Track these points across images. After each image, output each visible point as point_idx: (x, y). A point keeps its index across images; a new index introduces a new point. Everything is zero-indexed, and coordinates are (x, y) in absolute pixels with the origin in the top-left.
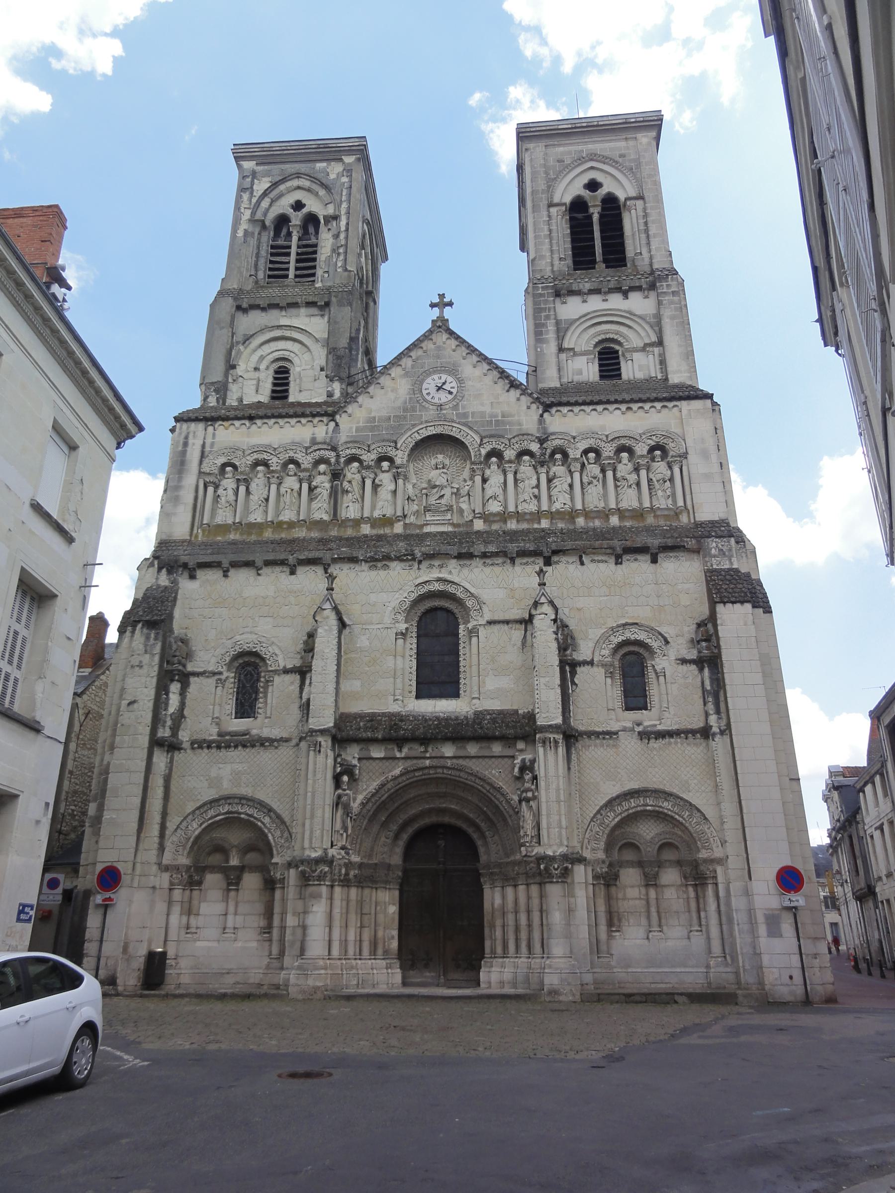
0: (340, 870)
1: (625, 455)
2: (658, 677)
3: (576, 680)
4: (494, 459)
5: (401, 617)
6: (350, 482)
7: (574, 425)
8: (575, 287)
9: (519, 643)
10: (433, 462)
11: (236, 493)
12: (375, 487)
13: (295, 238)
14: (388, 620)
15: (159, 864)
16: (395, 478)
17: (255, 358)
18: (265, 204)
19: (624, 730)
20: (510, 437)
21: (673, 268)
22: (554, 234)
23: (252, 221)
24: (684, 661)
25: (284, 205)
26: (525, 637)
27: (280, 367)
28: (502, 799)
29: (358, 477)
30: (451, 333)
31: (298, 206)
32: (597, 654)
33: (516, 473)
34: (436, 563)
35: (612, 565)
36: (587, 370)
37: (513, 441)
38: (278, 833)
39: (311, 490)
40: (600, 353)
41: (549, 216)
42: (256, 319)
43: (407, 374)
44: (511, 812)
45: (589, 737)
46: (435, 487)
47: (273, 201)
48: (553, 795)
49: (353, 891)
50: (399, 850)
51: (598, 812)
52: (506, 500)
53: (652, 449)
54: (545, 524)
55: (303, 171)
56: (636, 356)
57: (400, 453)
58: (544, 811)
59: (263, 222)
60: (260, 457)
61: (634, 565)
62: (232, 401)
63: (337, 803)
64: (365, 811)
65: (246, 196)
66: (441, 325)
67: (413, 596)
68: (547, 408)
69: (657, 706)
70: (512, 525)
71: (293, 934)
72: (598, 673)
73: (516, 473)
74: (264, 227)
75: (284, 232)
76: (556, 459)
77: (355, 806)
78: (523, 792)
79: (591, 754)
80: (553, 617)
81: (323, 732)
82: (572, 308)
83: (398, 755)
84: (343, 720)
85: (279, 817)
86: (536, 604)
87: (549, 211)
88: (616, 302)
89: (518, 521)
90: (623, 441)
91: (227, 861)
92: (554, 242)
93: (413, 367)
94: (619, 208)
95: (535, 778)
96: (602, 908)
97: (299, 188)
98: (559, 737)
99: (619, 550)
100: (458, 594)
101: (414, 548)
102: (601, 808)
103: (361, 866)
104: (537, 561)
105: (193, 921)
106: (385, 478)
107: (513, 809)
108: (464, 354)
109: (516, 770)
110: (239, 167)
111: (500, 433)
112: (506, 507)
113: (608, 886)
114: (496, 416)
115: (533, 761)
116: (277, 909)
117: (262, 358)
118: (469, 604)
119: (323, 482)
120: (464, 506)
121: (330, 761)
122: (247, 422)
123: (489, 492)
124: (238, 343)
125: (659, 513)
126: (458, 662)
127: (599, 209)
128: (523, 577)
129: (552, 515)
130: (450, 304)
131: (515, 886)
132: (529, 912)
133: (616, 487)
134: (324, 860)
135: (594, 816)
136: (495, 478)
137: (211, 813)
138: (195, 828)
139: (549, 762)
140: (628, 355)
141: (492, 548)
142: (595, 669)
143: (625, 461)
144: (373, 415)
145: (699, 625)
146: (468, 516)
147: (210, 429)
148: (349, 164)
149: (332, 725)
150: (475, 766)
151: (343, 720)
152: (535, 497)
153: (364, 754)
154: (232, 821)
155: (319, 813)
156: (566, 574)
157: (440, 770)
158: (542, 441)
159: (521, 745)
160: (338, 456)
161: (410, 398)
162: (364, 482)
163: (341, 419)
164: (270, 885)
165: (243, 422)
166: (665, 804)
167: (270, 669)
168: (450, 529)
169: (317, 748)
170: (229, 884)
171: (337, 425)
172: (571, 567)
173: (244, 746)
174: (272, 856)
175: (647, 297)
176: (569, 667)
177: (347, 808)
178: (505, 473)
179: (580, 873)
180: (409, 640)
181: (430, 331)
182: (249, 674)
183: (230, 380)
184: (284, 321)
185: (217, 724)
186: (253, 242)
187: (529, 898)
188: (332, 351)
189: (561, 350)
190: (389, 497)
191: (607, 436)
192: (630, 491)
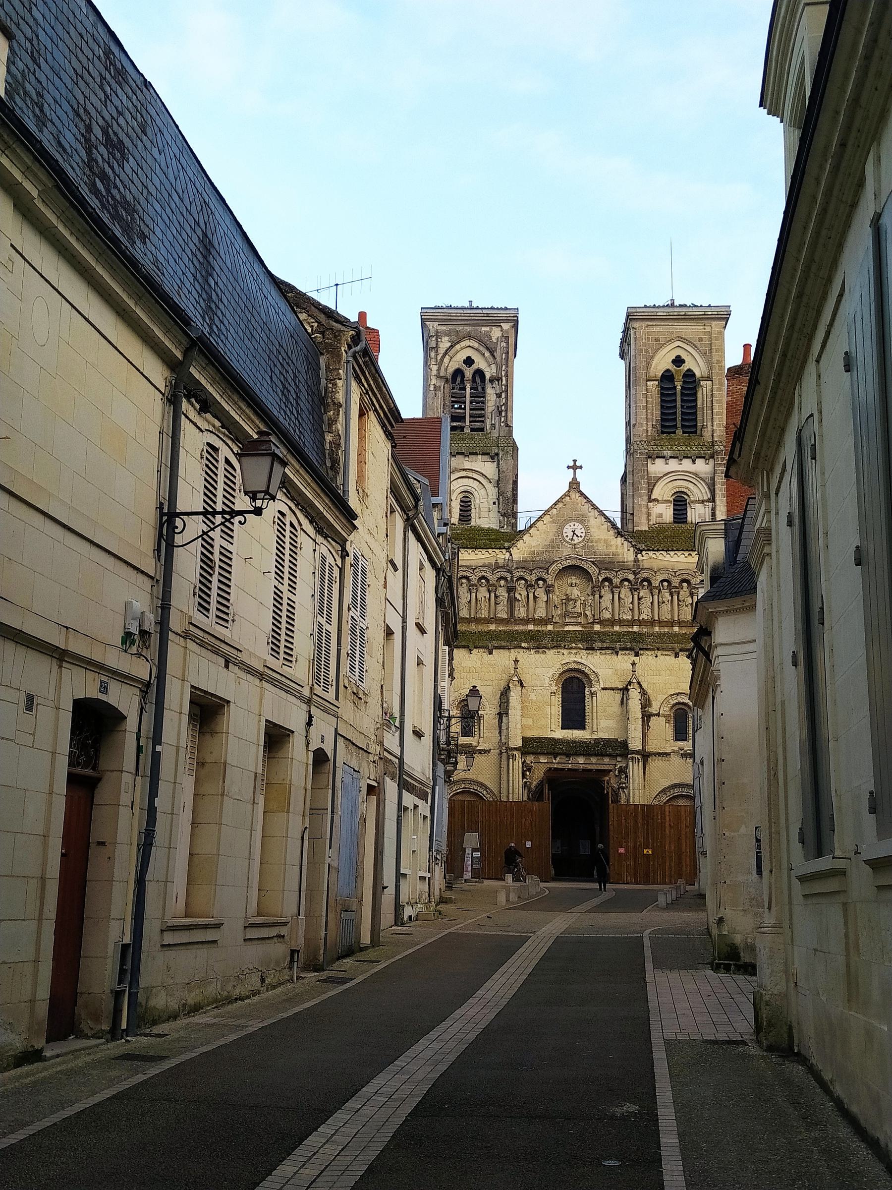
1: (685, 585)
4: (607, 583)
5: (553, 684)
12: (535, 598)
13: (468, 390)
16: (547, 592)
18: (447, 359)
26: (623, 698)
29: (524, 593)
30: (582, 494)
31: (469, 361)
36: (665, 513)
39: (496, 597)
43: (553, 522)
48: (636, 786)
54: (636, 629)
56: (698, 506)
65: (433, 354)
66: (574, 485)
70: (617, 628)
72: (662, 720)
74: (447, 381)
75: (459, 379)
77: (532, 787)
79: (655, 764)
81: (516, 749)
82: (657, 467)
86: (630, 683)
88: (687, 465)
95: (627, 777)
101: (560, 641)
106: (541, 593)
110: (424, 326)
112: (613, 615)
115: (627, 767)
119: (503, 593)
120: (588, 613)
123: (603, 605)
129: (641, 623)
130: (581, 467)
133: (679, 605)
136: (607, 596)
139: (635, 770)
140: (692, 505)
143: (685, 589)
148: (507, 331)
151: (525, 739)
153: (536, 760)
158: (635, 574)
159: (619, 759)
160: (512, 577)
163: (514, 551)
176: (647, 717)
177: (529, 789)
178: (613, 593)
181: (569, 491)
184: (467, 465)
186: (440, 394)
189: (650, 500)
191: (675, 572)
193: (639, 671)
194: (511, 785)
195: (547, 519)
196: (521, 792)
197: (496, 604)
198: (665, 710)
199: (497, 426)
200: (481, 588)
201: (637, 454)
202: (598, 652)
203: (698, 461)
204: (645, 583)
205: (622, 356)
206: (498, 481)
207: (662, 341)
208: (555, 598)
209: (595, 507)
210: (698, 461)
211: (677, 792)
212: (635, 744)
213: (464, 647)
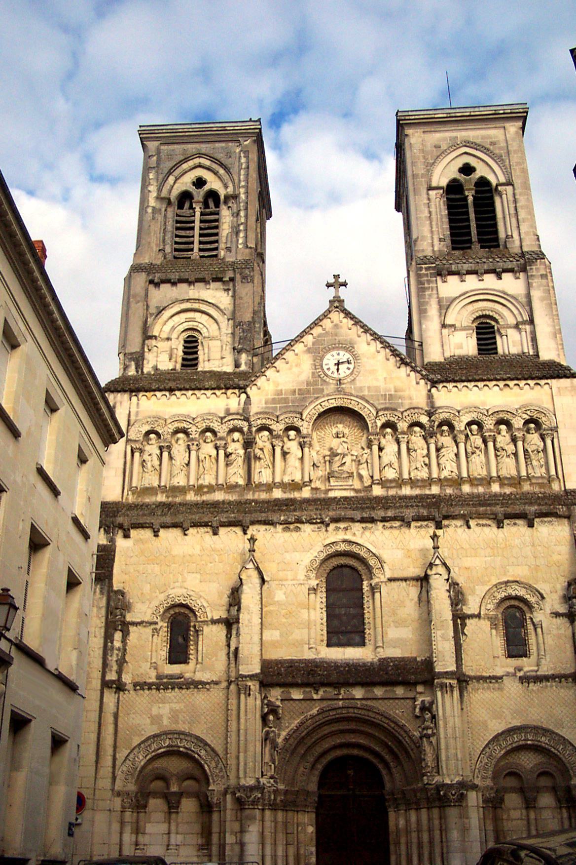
0: (270, 796)
1: (503, 427)
2: (535, 629)
3: (465, 631)
4: (389, 430)
5: (313, 575)
6: (261, 449)
7: (456, 399)
8: (454, 268)
9: (416, 599)
10: (334, 431)
11: (160, 458)
12: (285, 454)
13: (198, 214)
14: (301, 576)
15: (113, 790)
16: (302, 446)
17: (167, 328)
18: (171, 179)
19: (508, 674)
20: (402, 410)
21: (541, 251)
22: (434, 216)
23: (158, 198)
24: (557, 615)
25: (186, 183)
27: (188, 337)
28: (404, 735)
30: (348, 314)
31: (200, 183)
32: (483, 608)
33: (408, 442)
34: (342, 525)
35: (495, 529)
36: (465, 345)
37: (405, 414)
38: (214, 764)
39: (227, 455)
40: (477, 328)
41: (429, 199)
42: (167, 292)
43: (309, 351)
44: (413, 746)
45: (478, 681)
46: (337, 455)
47: (177, 179)
49: (280, 815)
50: (315, 779)
51: (487, 745)
52: (400, 467)
53: (527, 422)
54: (435, 490)
55: (203, 151)
57: (305, 424)
58: (443, 746)
59: (169, 199)
60: (181, 425)
61: (514, 529)
62: (148, 368)
63: (266, 738)
64: (287, 745)
66: (337, 304)
67: (323, 556)
68: (434, 383)
69: (535, 654)
71: (232, 850)
72: (485, 624)
73: (408, 442)
74: (170, 203)
76: (443, 431)
77: (280, 740)
78: (423, 729)
79: (479, 696)
80: (447, 577)
81: (252, 677)
82: (451, 287)
83: (315, 697)
84: (266, 665)
85: (213, 750)
86: (431, 565)
87: (428, 194)
88: (490, 281)
89: (412, 488)
90: (501, 415)
91: (168, 787)
92: (434, 223)
93: (313, 344)
94: (490, 191)
95: (434, 717)
96: (490, 827)
97: (200, 166)
98: (454, 682)
99: (500, 516)
100: (362, 553)
102: (489, 742)
103: (286, 792)
104: (430, 524)
105: (141, 839)
106: (293, 446)
107: (414, 743)
108: (359, 333)
109: (417, 710)
111: (393, 406)
112: (401, 474)
113: (495, 808)
114: (390, 390)
115: (432, 703)
116: (215, 829)
117: (173, 328)
118: (372, 562)
119: (237, 448)
120: (364, 473)
121: (259, 702)
122: (167, 393)
124: (151, 315)
125: (534, 481)
126: (363, 614)
127: (473, 192)
128: (418, 538)
130: (345, 284)
131: (417, 809)
132: (430, 830)
133: (496, 456)
134: (258, 787)
135: (483, 750)
136: (391, 448)
137: (154, 746)
138: (141, 759)
139: (447, 705)
140: (503, 331)
141: (390, 513)
142: (482, 621)
143: (504, 433)
144: (279, 388)
145: (569, 584)
146: (368, 482)
147: (134, 399)
149: (258, 671)
150: (381, 706)
151: (266, 665)
152: (426, 465)
154: (172, 753)
155: (251, 748)
156: (455, 534)
157: (351, 710)
158: (430, 414)
159: (420, 688)
160: (250, 426)
161: (313, 373)
162: (274, 450)
164: (207, 807)
165: (164, 393)
166: (543, 739)
167: (199, 619)
168: (352, 494)
169: (248, 692)
170: (170, 808)
171: (248, 397)
172: (460, 531)
173: (180, 688)
174: (208, 784)
175: (518, 278)
176: (460, 619)
178: (398, 442)
179: (473, 798)
180: (319, 594)
182: (181, 624)
183: (146, 350)
185: (156, 668)
186: (160, 218)
187: (430, 819)
188: (237, 324)
189: (444, 326)
190: (298, 464)
192: (508, 460)
193: (443, 552)
194: (242, 738)
195: (299, 347)
196: (259, 749)
197: (227, 465)
198: (490, 606)
199: (233, 249)
200: (203, 445)
201: (424, 270)
202: (380, 525)
203: (504, 275)
204: (445, 428)
205: (398, 208)
206: (234, 312)
207: (444, 147)
208: (314, 454)
209: (367, 330)
210: (504, 275)
211: (517, 739)
212: (445, 663)
213: (175, 526)
